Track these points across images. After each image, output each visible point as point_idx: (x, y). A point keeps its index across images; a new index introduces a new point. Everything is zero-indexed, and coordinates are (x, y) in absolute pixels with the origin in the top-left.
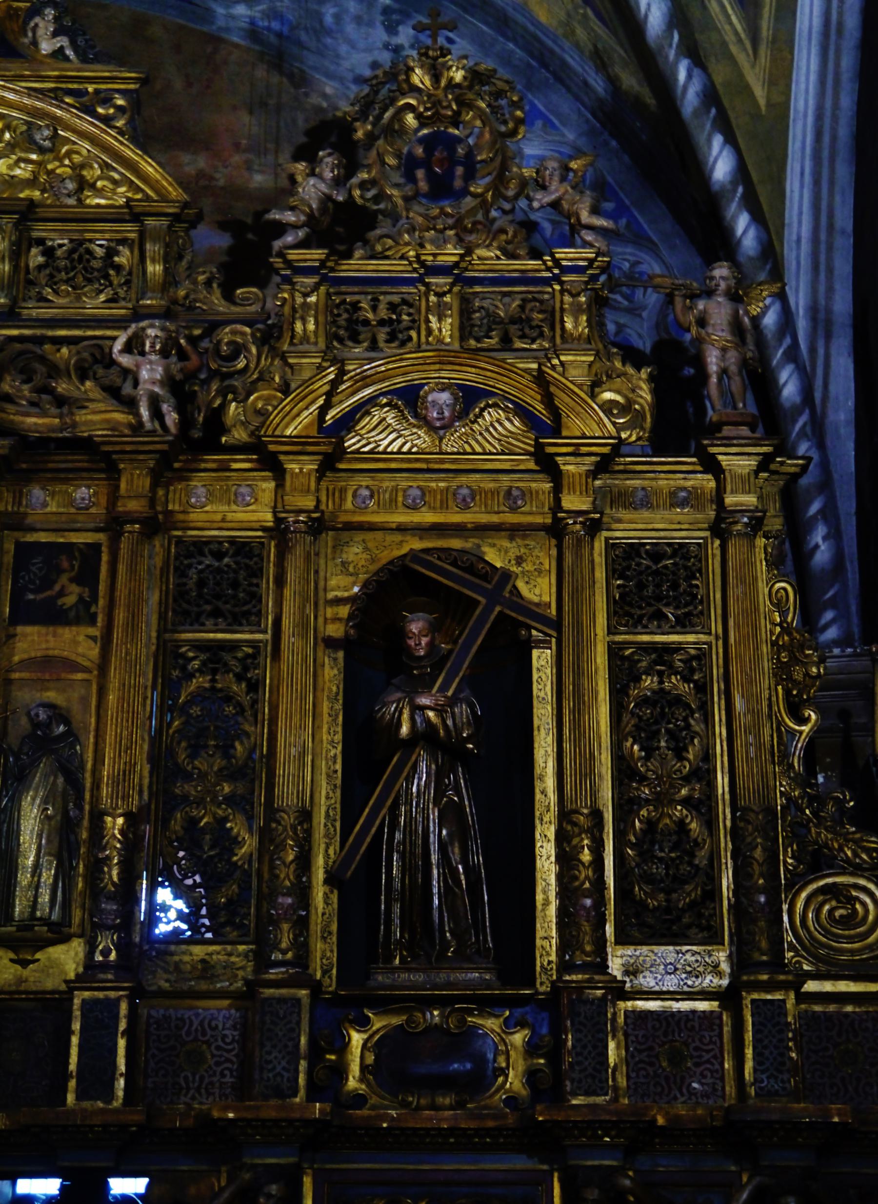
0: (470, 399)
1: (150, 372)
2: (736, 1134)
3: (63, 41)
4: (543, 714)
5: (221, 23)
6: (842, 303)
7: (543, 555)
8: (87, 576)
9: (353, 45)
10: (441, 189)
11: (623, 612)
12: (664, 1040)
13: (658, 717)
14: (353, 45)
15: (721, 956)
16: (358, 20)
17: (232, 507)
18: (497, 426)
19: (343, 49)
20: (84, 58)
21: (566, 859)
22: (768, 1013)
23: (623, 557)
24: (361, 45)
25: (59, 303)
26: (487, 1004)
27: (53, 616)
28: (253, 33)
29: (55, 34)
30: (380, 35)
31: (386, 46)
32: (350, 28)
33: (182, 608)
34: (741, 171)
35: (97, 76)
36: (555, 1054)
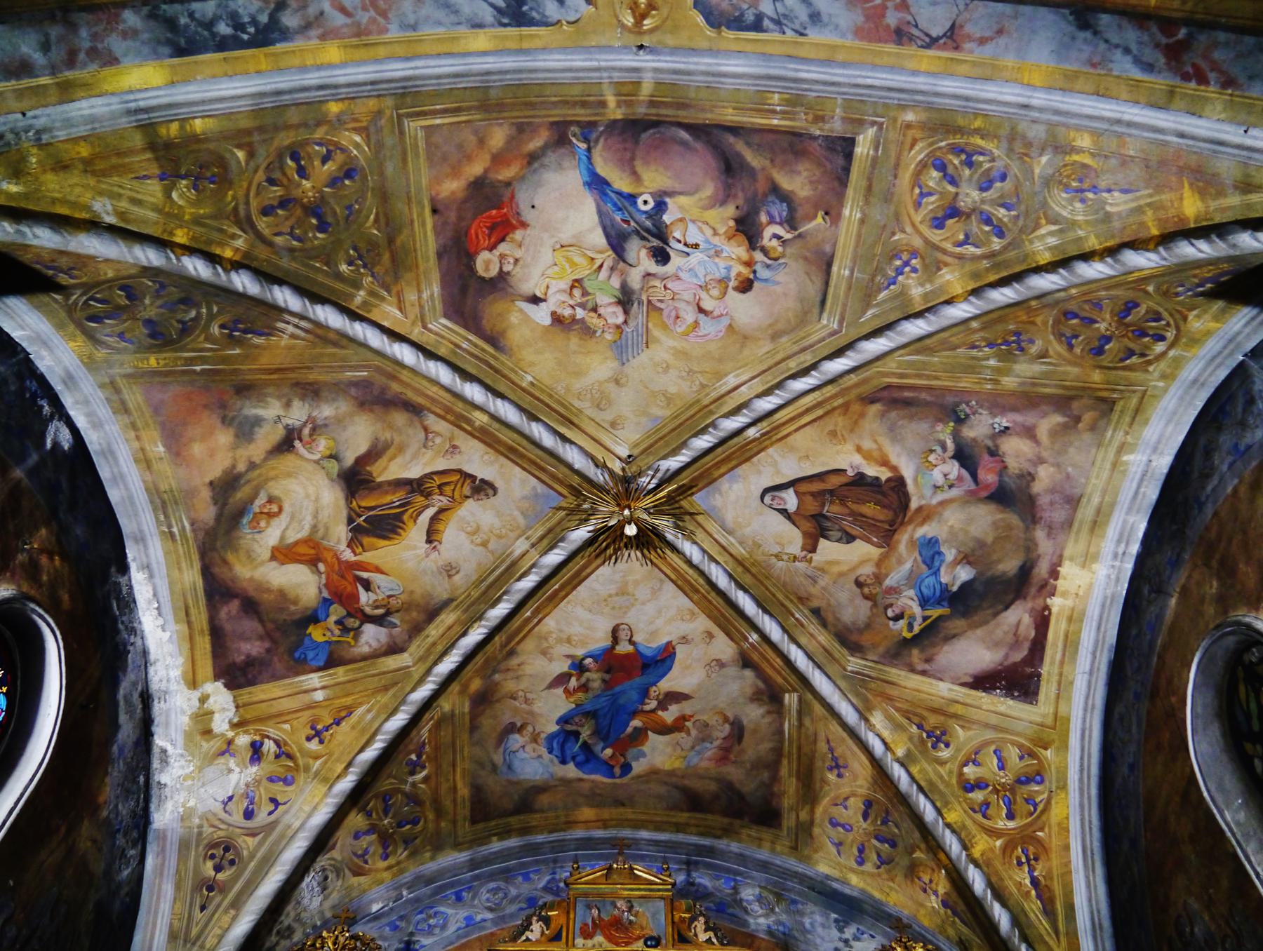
3: (711, 934)
5: (753, 927)
9: (823, 939)
14: (823, 939)
16: (823, 926)
19: (818, 941)
20: (722, 944)
24: (827, 939)
28: (770, 932)
29: (706, 931)
30: (835, 933)
31: (840, 939)
32: (820, 930)
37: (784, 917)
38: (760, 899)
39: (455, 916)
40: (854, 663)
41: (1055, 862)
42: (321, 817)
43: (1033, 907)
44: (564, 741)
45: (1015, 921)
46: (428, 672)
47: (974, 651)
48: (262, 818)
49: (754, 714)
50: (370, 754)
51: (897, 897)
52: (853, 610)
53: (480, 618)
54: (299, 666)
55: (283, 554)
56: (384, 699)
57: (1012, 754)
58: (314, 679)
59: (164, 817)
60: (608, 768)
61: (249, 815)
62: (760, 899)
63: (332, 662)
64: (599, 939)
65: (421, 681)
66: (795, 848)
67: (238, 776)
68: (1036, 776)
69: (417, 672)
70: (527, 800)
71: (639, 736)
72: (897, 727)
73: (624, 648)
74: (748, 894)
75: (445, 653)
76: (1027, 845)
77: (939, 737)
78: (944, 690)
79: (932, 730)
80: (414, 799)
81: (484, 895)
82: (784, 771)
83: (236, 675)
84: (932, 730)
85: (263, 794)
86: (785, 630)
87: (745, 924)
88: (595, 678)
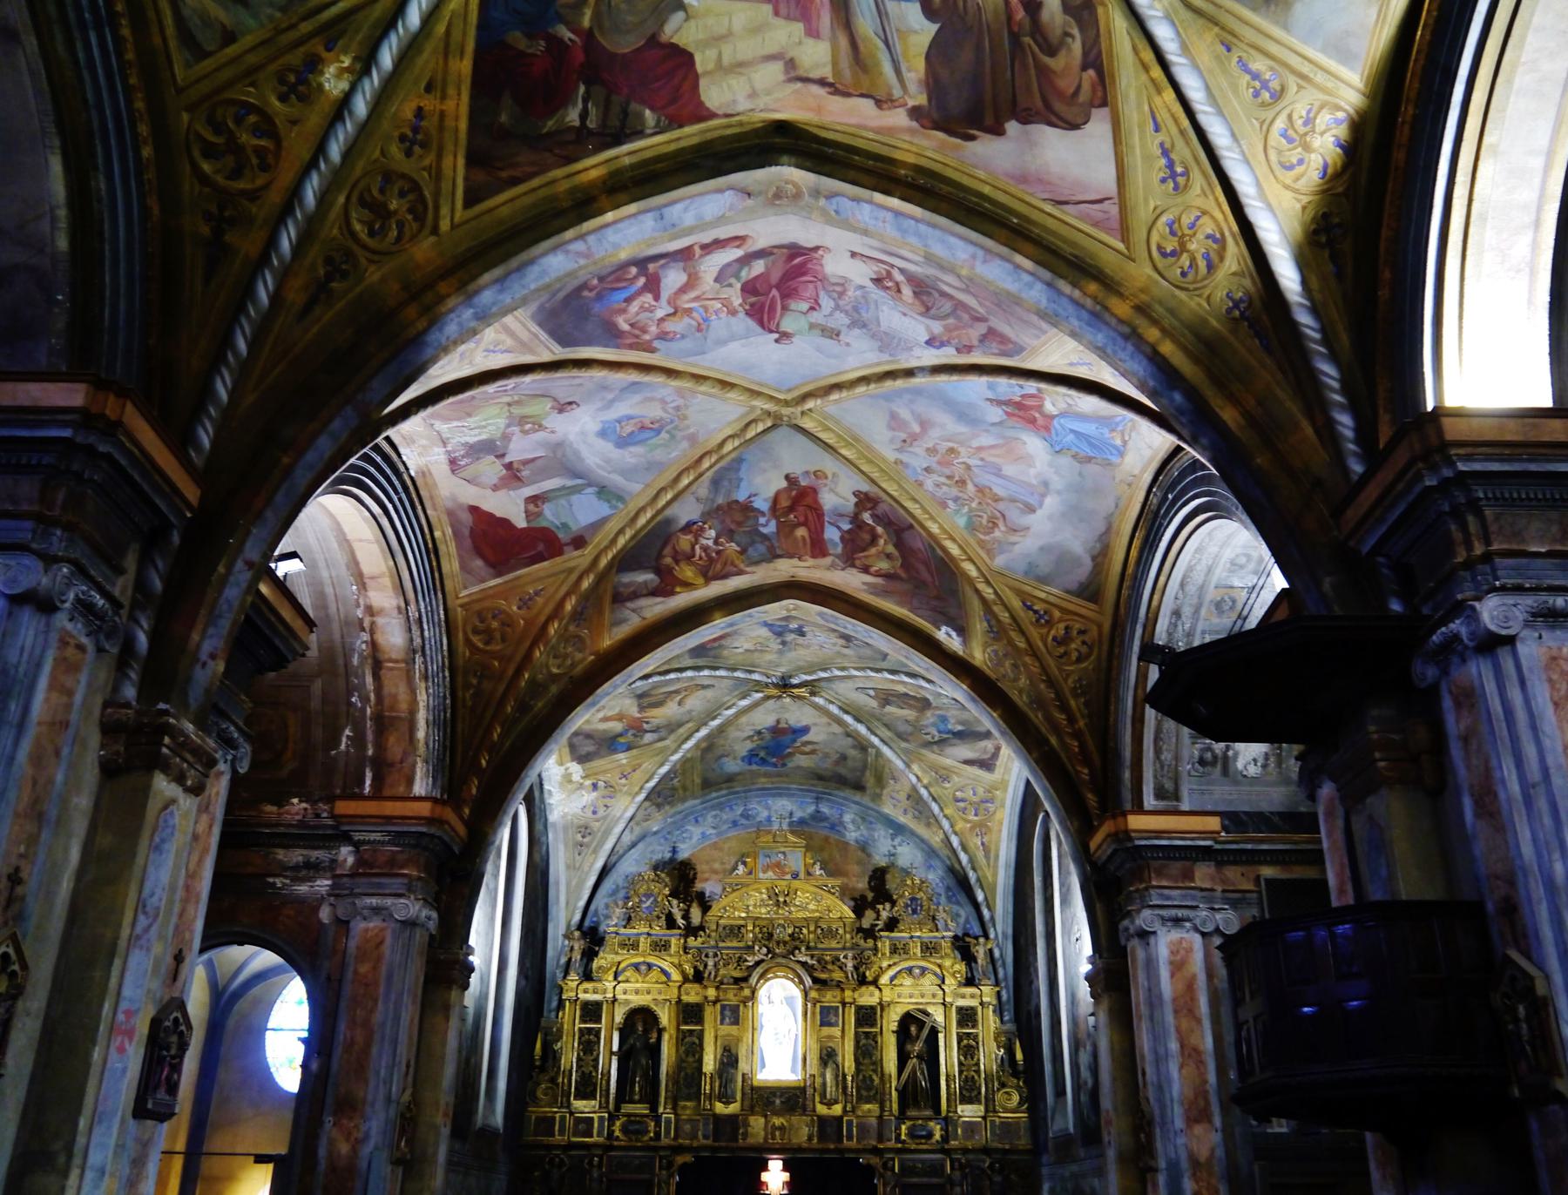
0: (924, 970)
1: (850, 965)
2: (986, 1150)
4: (942, 1049)
6: (1010, 931)
7: (941, 1009)
8: (837, 1015)
10: (914, 911)
11: (960, 1024)
12: (971, 1128)
13: (968, 1049)
15: (982, 1108)
17: (869, 997)
18: (929, 982)
21: (948, 1086)
22: (993, 1122)
23: (960, 1010)
25: (827, 944)
26: (931, 1119)
27: (830, 1025)
33: (859, 1023)
34: (986, 898)
35: (831, 882)
36: (947, 1131)
37: (865, 832)
38: (853, 822)
39: (696, 831)
40: (904, 745)
41: (994, 836)
42: (629, 814)
43: (980, 855)
44: (751, 757)
45: (971, 860)
46: (679, 746)
47: (965, 751)
48: (601, 812)
49: (853, 753)
50: (652, 784)
51: (921, 830)
52: (902, 728)
53: (705, 724)
54: (615, 751)
55: (605, 719)
56: (658, 759)
57: (980, 791)
58: (621, 756)
59: (554, 816)
60: (775, 765)
61: (594, 813)
62: (853, 822)
63: (629, 748)
64: (770, 874)
65: (675, 751)
66: (873, 800)
67: (588, 797)
68: (991, 801)
69: (674, 746)
70: (730, 779)
71: (791, 755)
72: (924, 771)
73: (783, 725)
74: (847, 818)
75: (687, 739)
76: (982, 828)
77: (946, 779)
78: (948, 762)
79: (943, 775)
80: (674, 789)
81: (710, 819)
82: (868, 773)
83: (582, 759)
84: (943, 775)
85: (600, 803)
86: (869, 729)
87: (843, 836)
88: (768, 736)
